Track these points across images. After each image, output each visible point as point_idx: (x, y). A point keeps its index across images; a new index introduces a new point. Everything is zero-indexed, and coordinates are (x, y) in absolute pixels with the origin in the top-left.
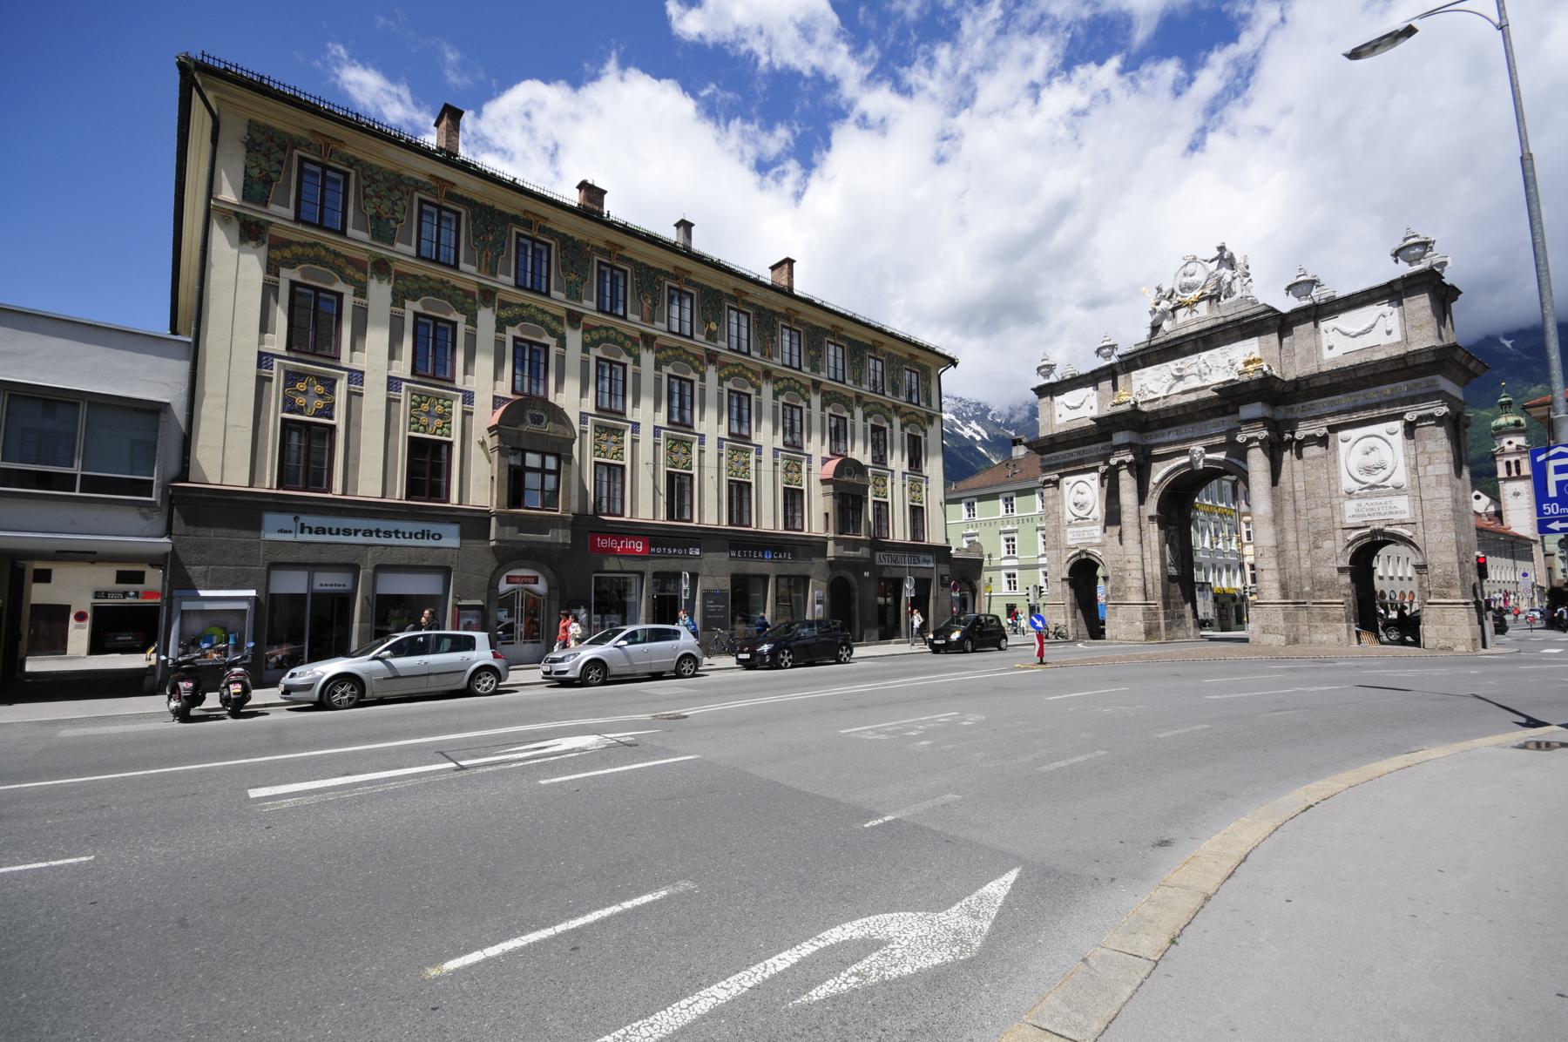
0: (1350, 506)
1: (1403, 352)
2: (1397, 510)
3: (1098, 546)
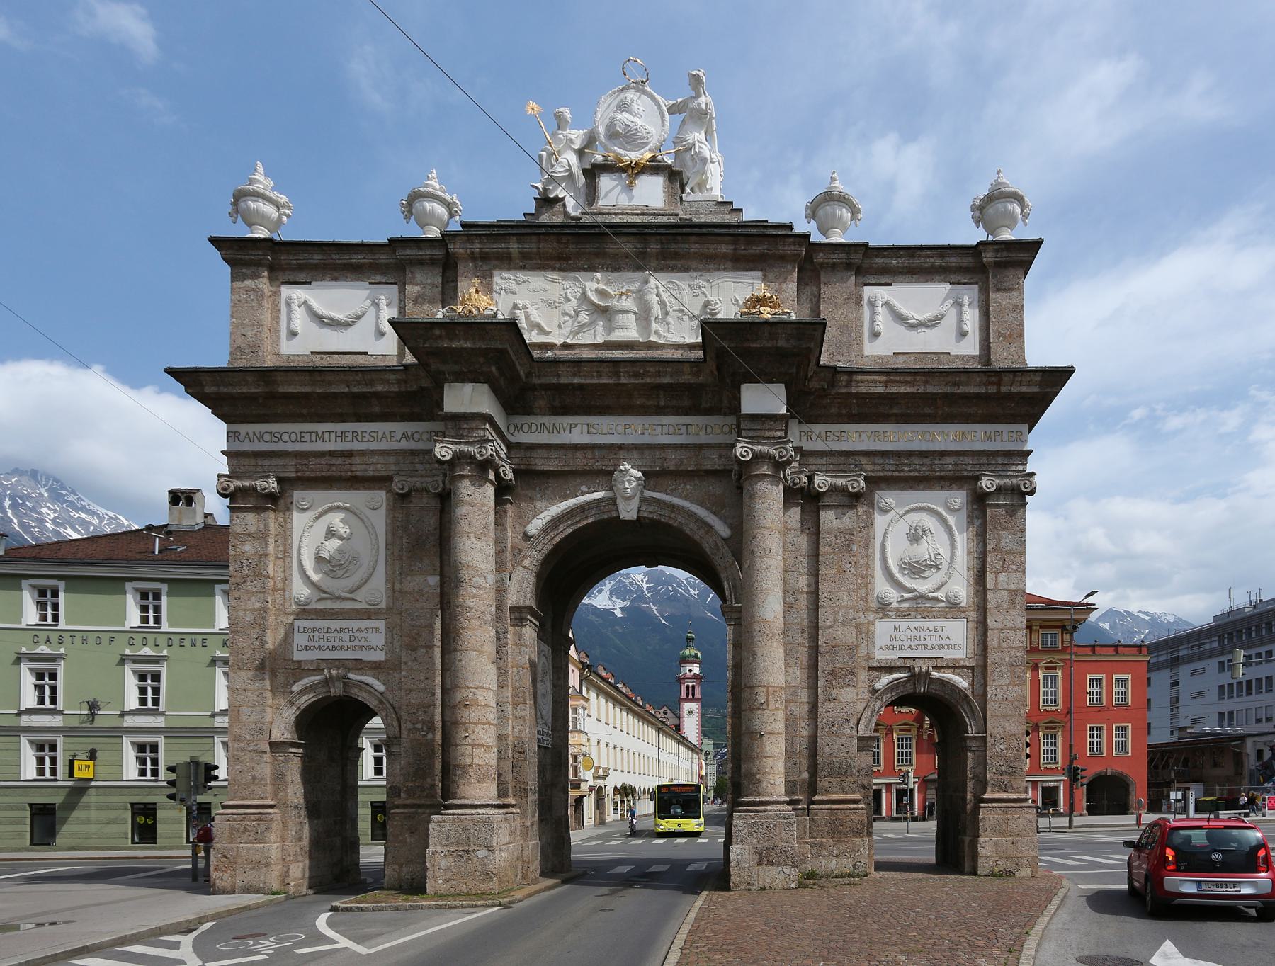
0: (883, 629)
2: (953, 639)
3: (376, 667)
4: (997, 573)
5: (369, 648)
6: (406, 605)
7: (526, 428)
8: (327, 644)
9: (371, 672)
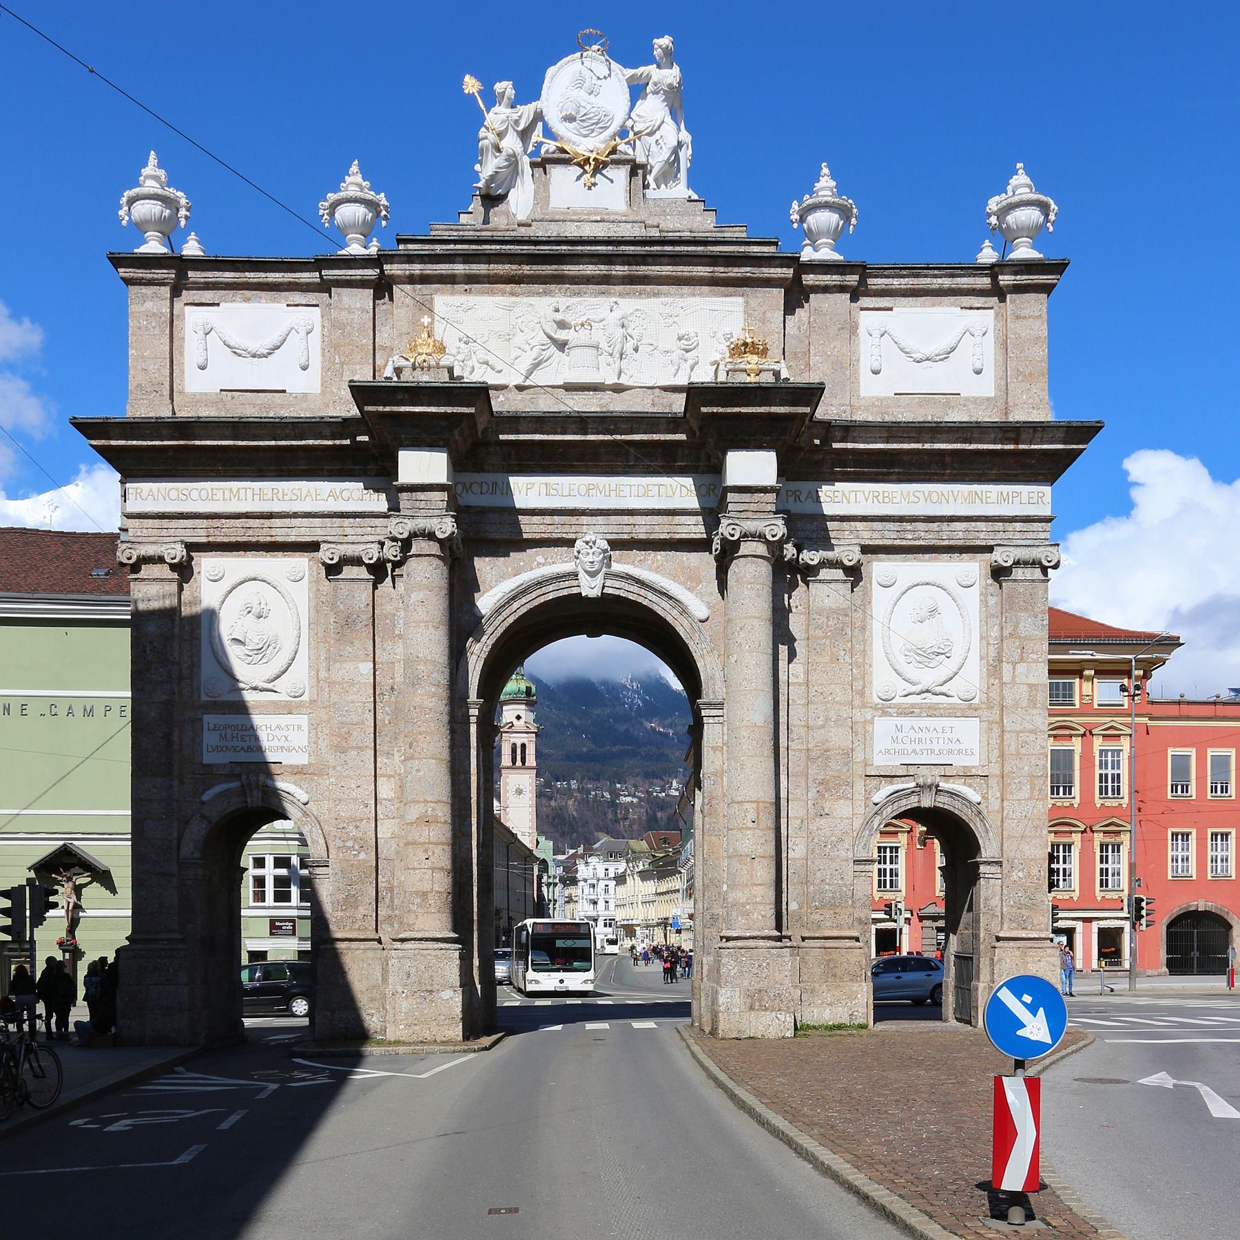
0: (883, 728)
1: (996, 418)
4: (1014, 664)
5: (289, 750)
6: (335, 698)
7: (476, 488)
8: (241, 744)
9: (293, 778)
